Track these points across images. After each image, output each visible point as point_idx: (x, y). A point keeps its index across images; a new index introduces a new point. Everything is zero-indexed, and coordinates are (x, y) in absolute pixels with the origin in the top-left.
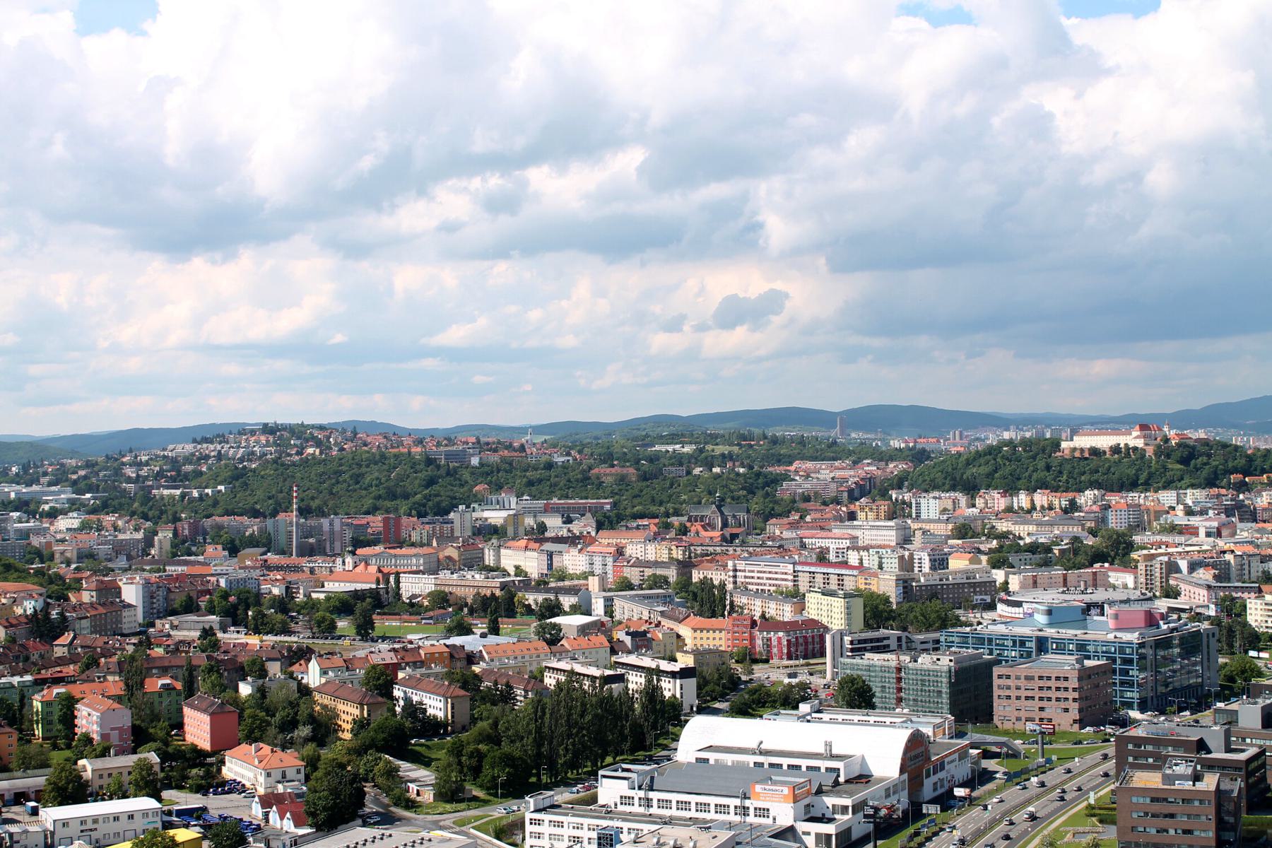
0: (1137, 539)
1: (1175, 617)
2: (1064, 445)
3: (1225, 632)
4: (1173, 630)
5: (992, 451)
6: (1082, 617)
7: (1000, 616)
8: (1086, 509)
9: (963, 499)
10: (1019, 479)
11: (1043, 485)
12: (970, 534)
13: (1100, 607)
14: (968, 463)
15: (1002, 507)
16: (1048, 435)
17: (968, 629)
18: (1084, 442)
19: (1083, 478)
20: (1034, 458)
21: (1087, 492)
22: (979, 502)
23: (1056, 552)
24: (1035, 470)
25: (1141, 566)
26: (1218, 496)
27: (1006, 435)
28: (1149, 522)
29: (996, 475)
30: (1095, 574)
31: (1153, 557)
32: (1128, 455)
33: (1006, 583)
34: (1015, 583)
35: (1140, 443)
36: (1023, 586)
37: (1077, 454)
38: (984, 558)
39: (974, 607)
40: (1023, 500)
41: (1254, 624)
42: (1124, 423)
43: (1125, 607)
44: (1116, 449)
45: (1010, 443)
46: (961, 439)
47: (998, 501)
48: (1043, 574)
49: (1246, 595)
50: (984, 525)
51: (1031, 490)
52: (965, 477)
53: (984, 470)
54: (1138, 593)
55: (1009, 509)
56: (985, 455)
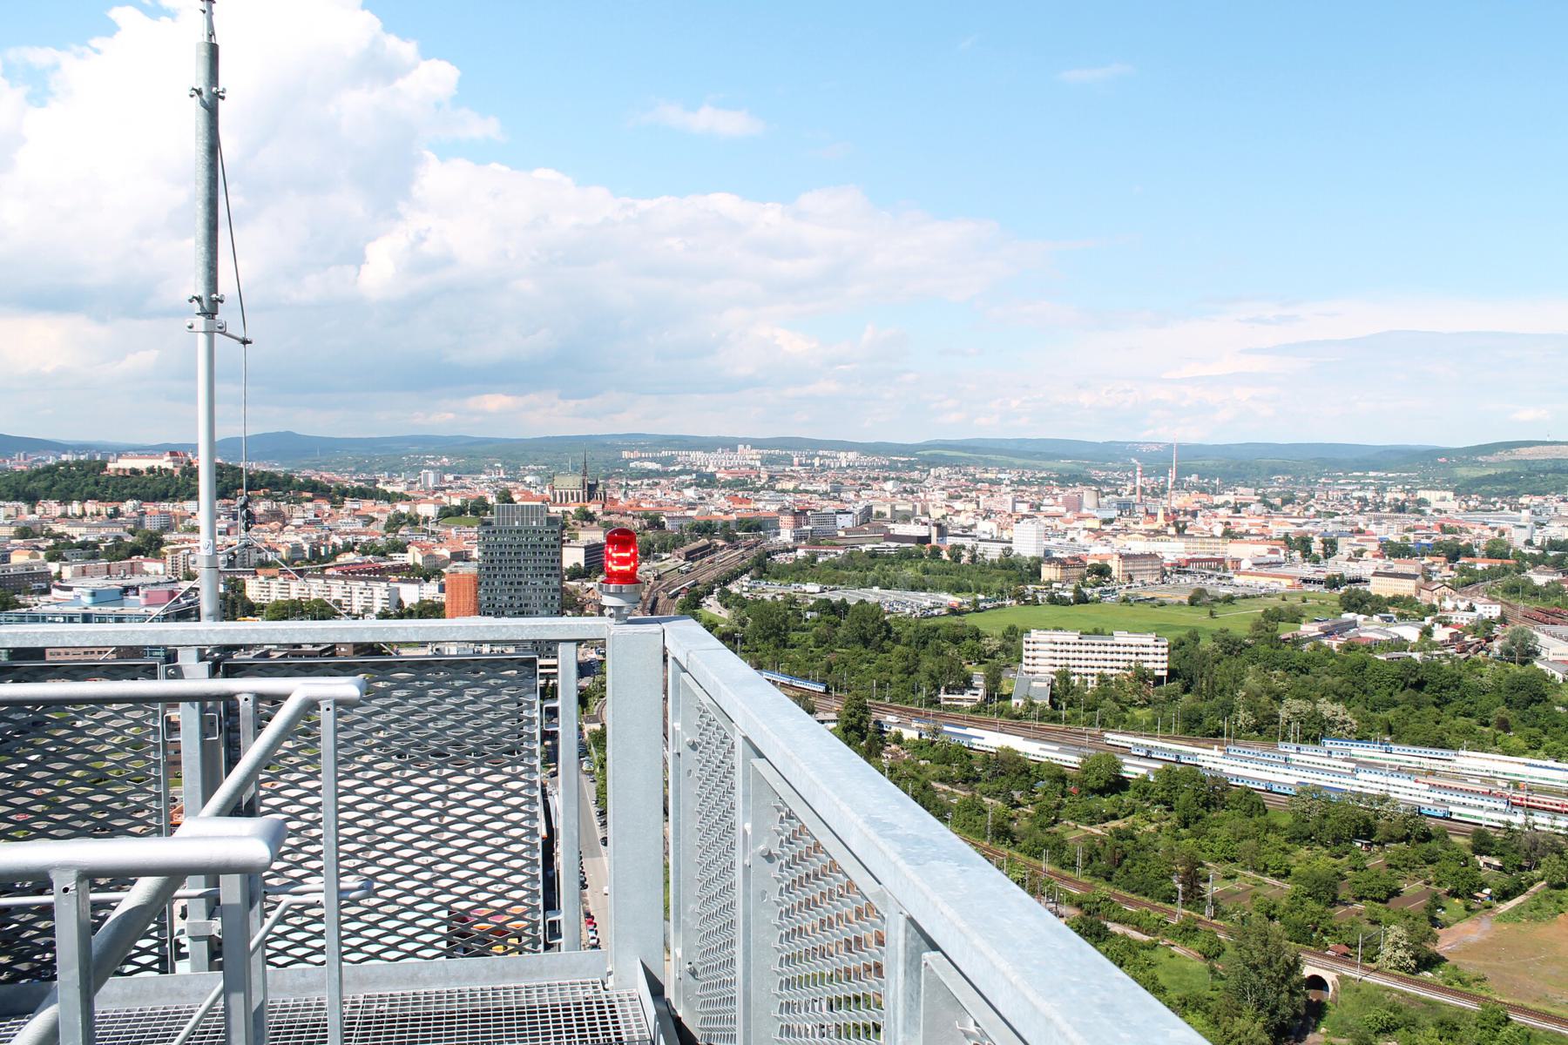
0: (166, 537)
1: (193, 594)
2: (110, 466)
3: (229, 604)
4: (190, 604)
5: (50, 470)
6: (120, 597)
7: (55, 599)
8: (127, 515)
9: (24, 507)
10: (72, 492)
11: (93, 496)
12: (31, 535)
13: (136, 589)
14: (30, 479)
15: (59, 513)
16: (98, 458)
17: (24, 610)
18: (126, 464)
19: (125, 491)
20: (85, 475)
21: (128, 502)
22: (39, 510)
23: (103, 548)
24: (87, 485)
25: (169, 558)
26: (228, 505)
27: (64, 458)
28: (176, 524)
29: (54, 488)
30: (132, 564)
31: (178, 550)
32: (160, 474)
33: (60, 573)
34: (67, 572)
35: (170, 466)
36: (74, 575)
37: (120, 473)
38: (42, 554)
39: (32, 593)
40: (75, 508)
41: (251, 598)
42: (160, 450)
43: (154, 588)
44: (151, 470)
45: (66, 464)
46: (25, 459)
47: (55, 509)
48: (91, 565)
49: (245, 577)
50: (43, 528)
51: (83, 500)
52: (27, 489)
53: (43, 484)
54: (166, 577)
55: (65, 515)
56: (45, 472)
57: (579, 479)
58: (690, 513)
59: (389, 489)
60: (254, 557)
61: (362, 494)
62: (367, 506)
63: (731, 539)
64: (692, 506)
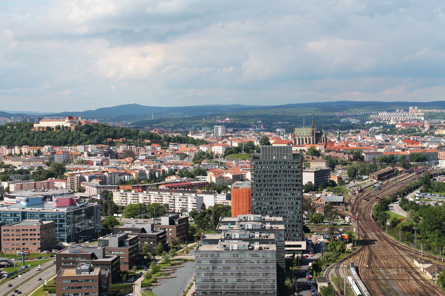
18: (44, 124)
34: (12, 188)
44: (58, 128)
48: (25, 183)
51: (20, 146)
55: (10, 155)
57: (310, 130)
58: (379, 150)
59: (195, 137)
60: (118, 178)
61: (180, 141)
62: (182, 148)
63: (406, 166)
64: (381, 146)
